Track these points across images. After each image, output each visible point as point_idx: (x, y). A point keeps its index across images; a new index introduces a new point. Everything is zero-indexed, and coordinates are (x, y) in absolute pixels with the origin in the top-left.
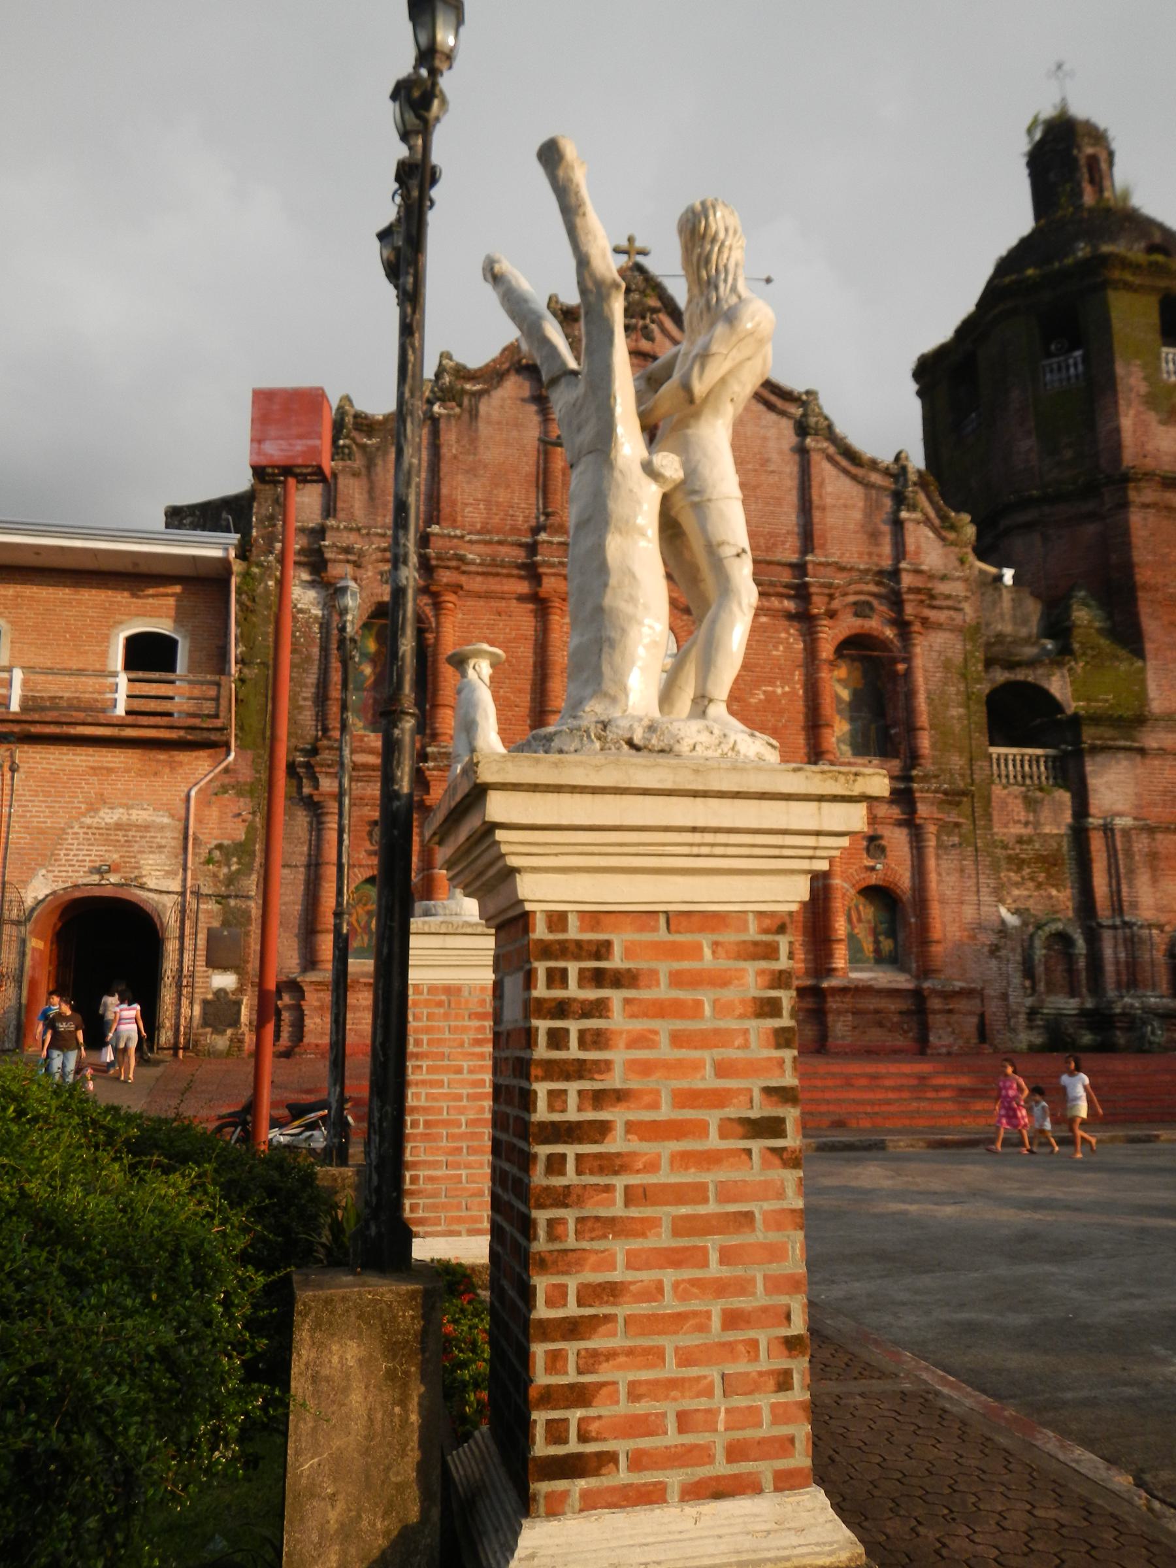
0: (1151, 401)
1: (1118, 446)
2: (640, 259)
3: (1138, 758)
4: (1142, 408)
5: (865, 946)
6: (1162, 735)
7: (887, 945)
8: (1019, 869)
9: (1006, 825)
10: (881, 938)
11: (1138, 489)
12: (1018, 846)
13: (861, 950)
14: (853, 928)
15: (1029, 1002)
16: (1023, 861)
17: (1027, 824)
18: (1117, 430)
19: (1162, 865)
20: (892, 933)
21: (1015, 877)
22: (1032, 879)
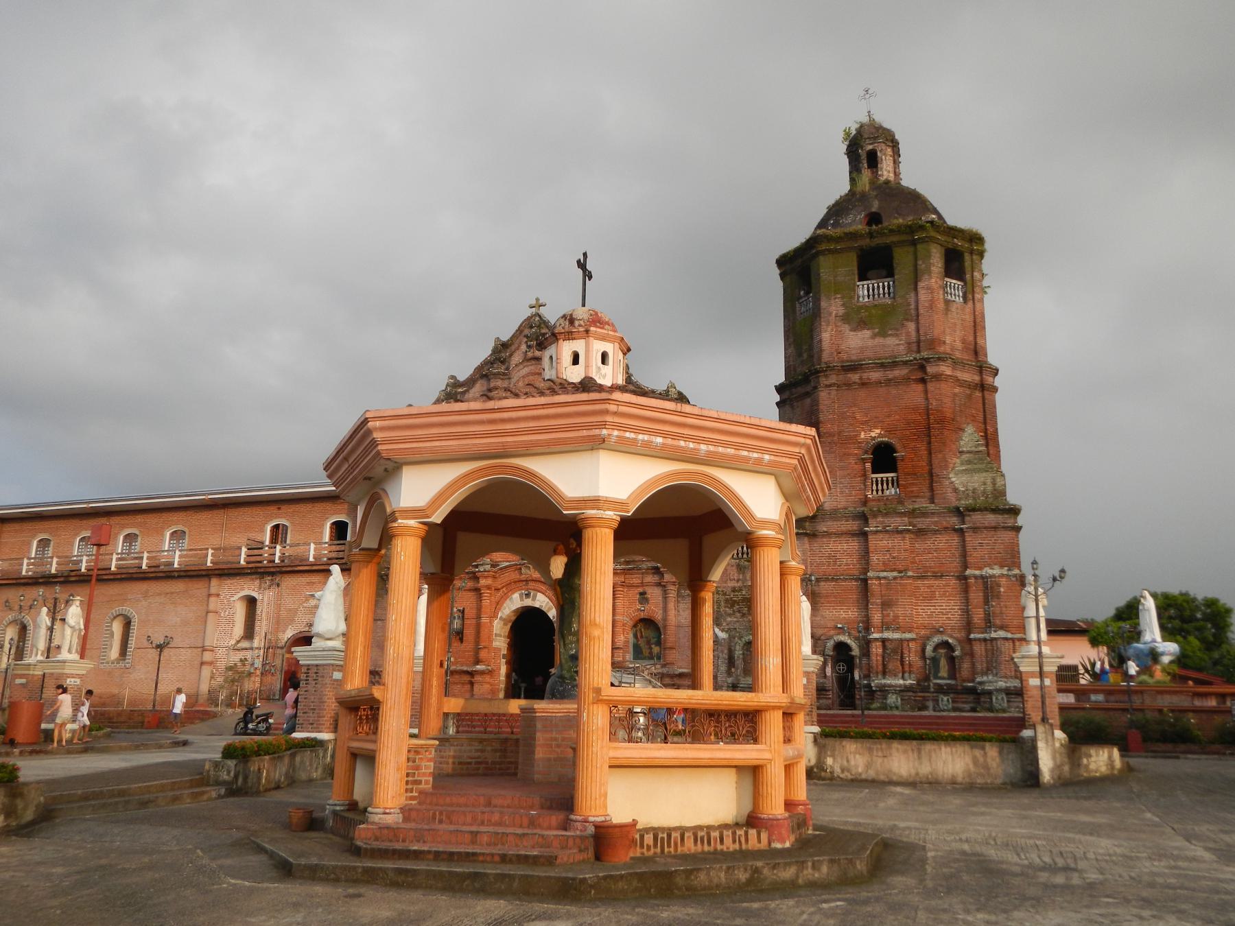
0: (846, 318)
1: (821, 351)
2: (542, 310)
3: (806, 539)
4: (840, 324)
5: (644, 651)
6: (829, 523)
7: (656, 649)
8: (732, 606)
9: (726, 582)
10: (653, 646)
11: (826, 376)
12: (732, 594)
13: (642, 653)
14: (638, 641)
15: (730, 680)
16: (735, 601)
17: (738, 581)
18: (820, 341)
19: (822, 600)
20: (659, 643)
21: (729, 611)
22: (739, 612)
